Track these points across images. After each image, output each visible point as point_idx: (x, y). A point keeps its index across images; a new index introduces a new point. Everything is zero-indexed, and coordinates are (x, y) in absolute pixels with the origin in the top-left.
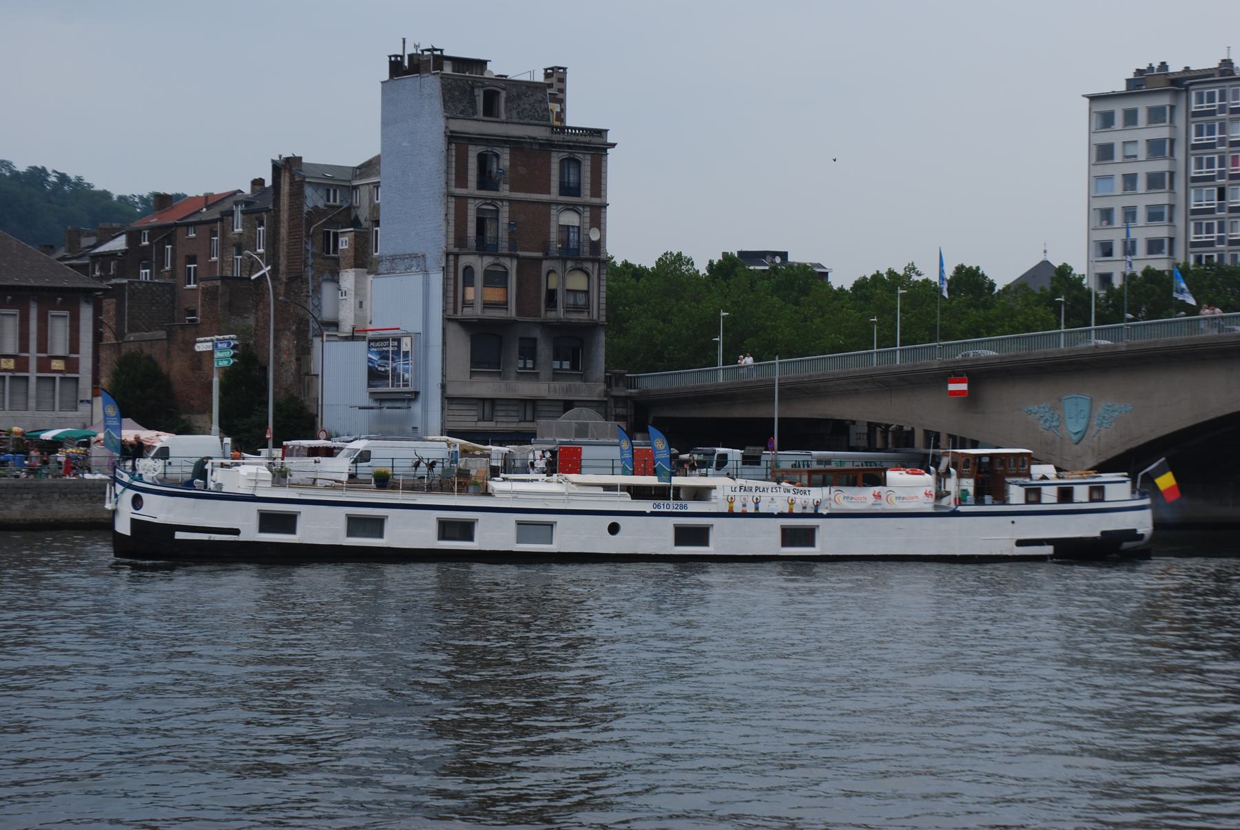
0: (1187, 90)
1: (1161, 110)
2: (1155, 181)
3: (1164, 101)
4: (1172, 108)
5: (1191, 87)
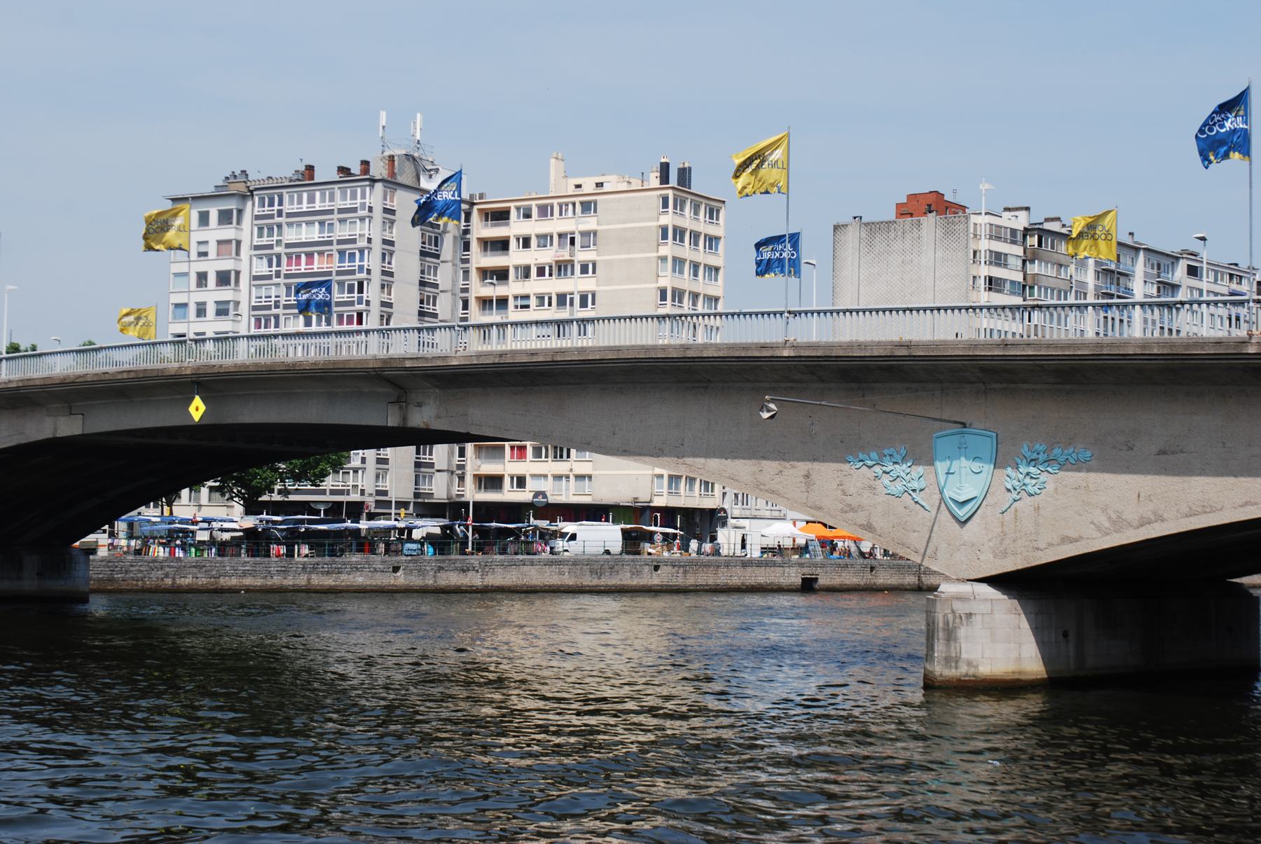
0: (252, 195)
1: (230, 212)
2: (224, 279)
3: (231, 205)
4: (240, 212)
5: (255, 193)
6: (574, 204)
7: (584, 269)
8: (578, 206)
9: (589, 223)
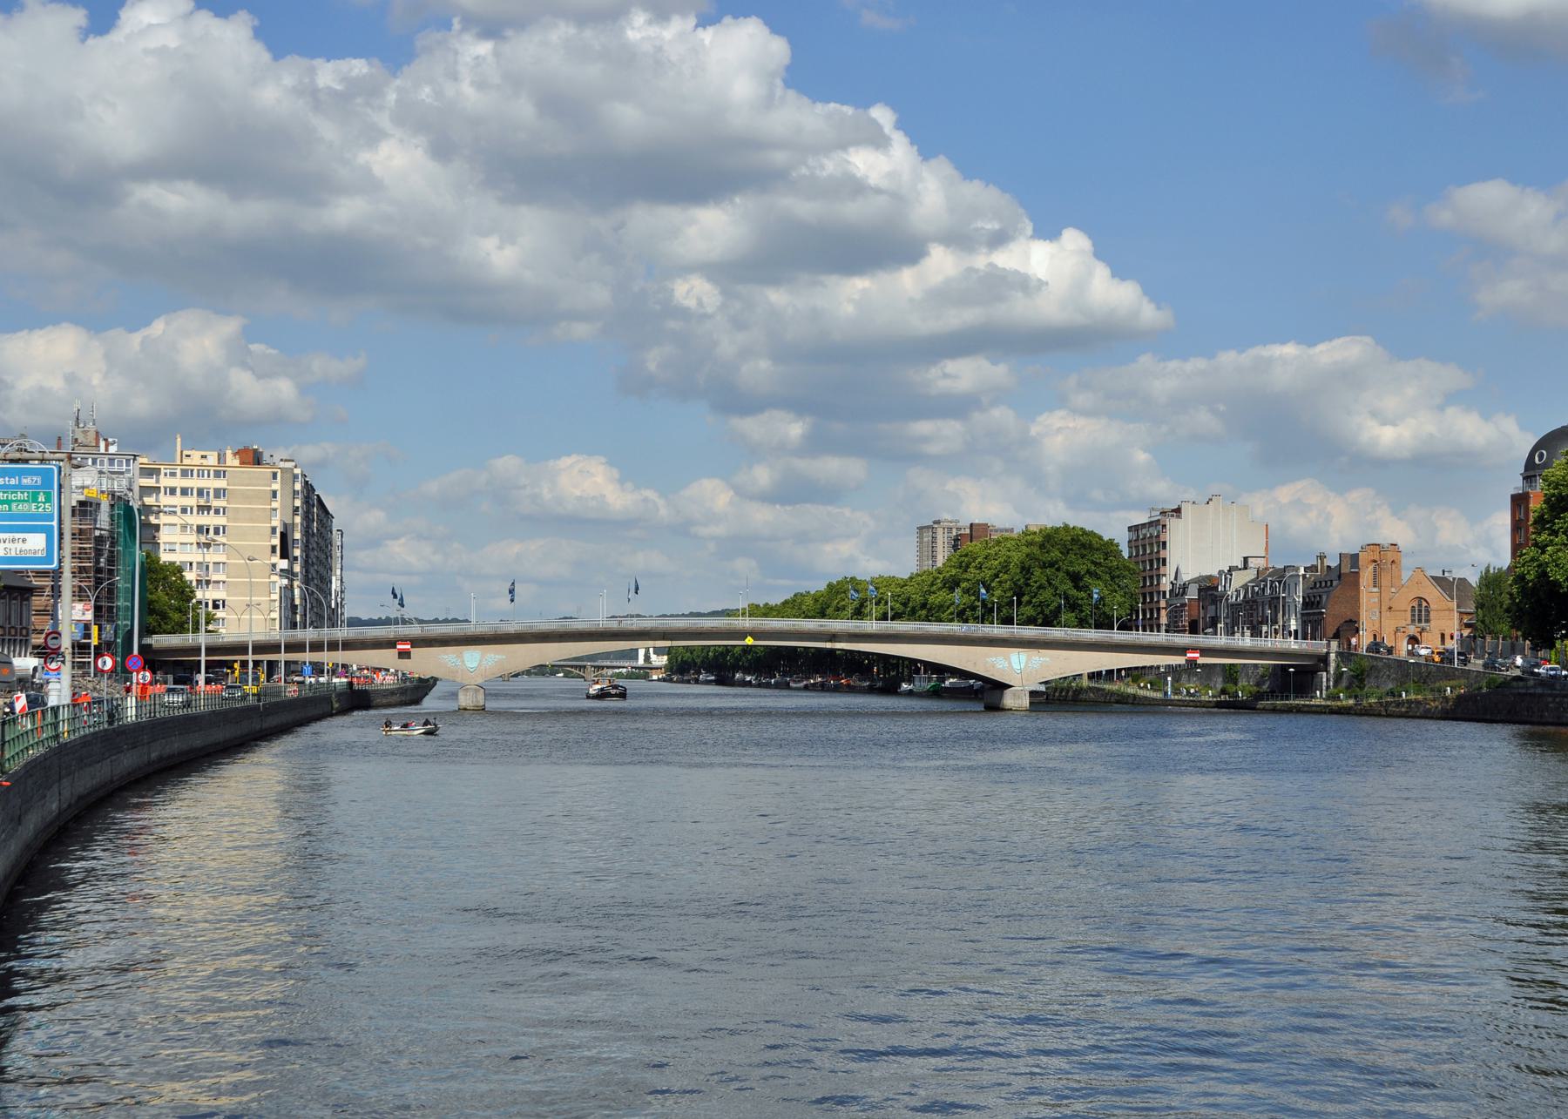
6: (209, 471)
7: (217, 512)
8: (212, 473)
9: (221, 483)
